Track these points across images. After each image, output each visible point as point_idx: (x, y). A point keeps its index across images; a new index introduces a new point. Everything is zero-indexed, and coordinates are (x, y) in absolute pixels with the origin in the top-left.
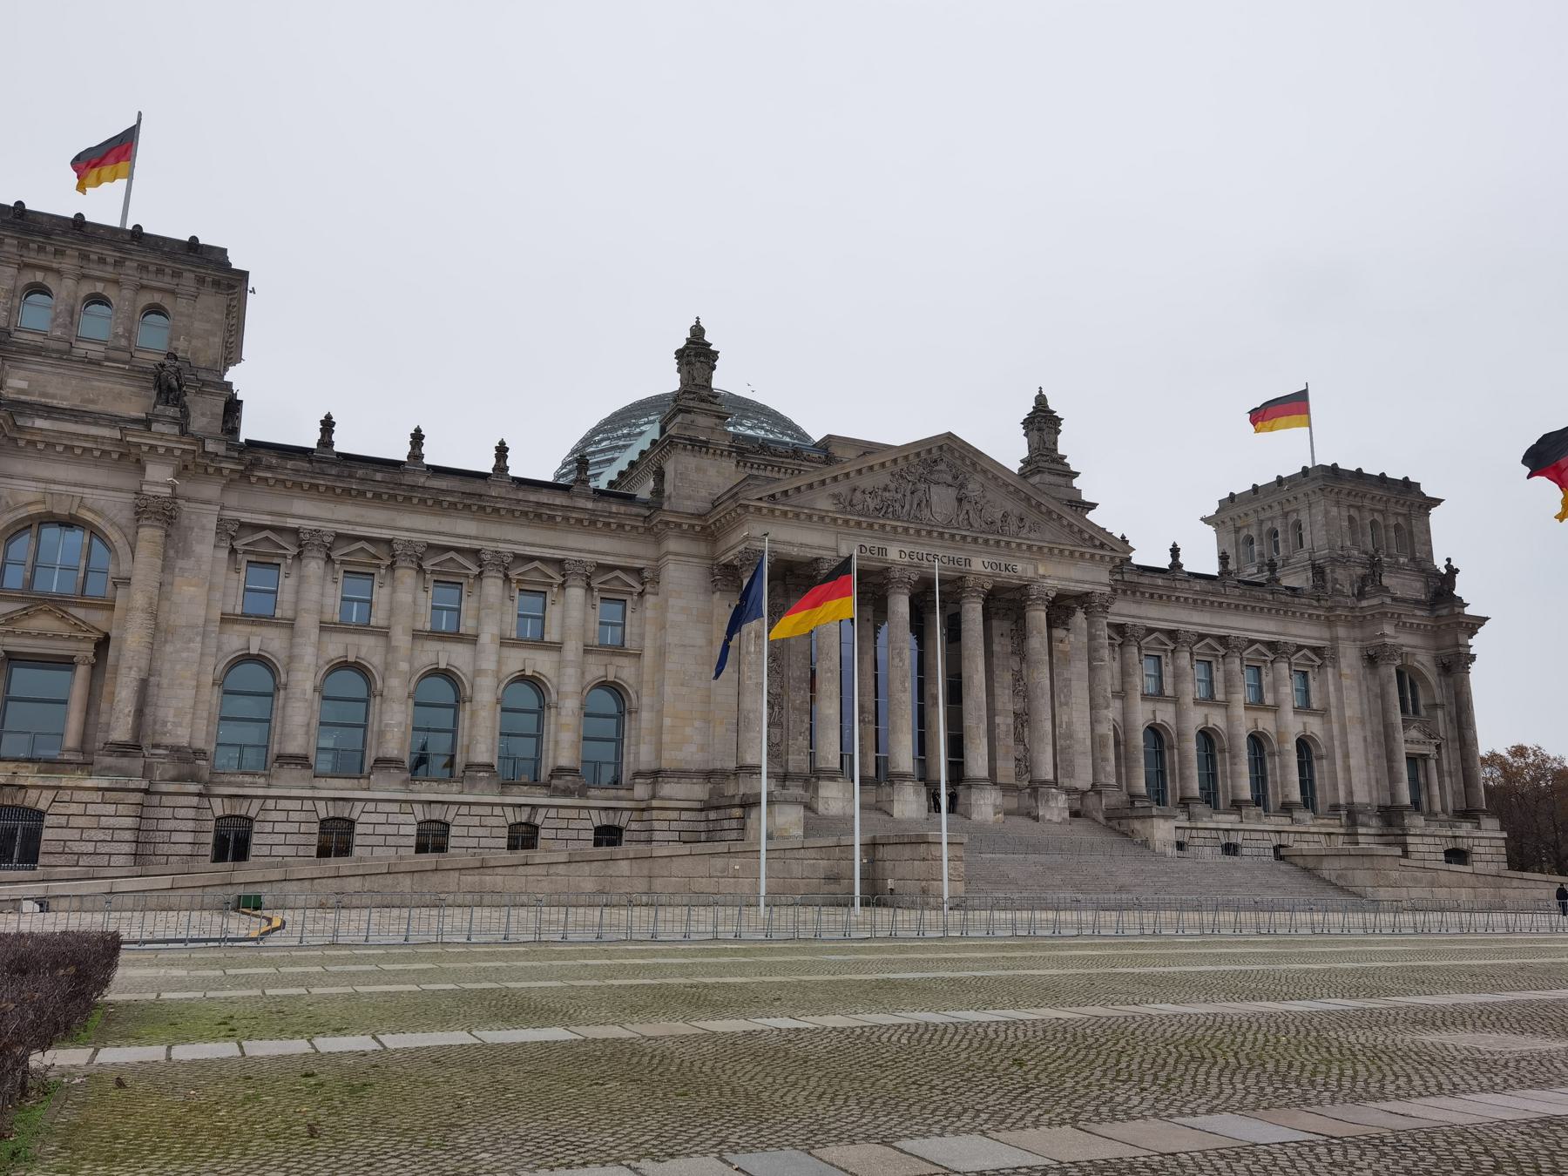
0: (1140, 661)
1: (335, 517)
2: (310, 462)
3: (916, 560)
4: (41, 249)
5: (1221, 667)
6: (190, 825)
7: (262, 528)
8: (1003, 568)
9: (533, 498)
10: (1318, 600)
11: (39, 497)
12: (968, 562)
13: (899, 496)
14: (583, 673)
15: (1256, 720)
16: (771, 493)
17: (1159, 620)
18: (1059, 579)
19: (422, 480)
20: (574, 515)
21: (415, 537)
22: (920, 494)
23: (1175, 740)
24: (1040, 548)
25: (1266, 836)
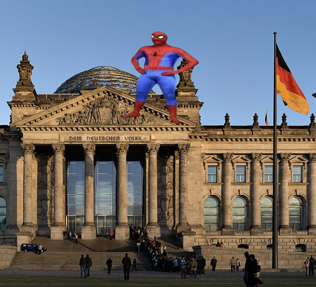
0: (233, 169)
3: (94, 140)
8: (135, 138)
15: (296, 191)
17: (242, 150)
18: (162, 140)
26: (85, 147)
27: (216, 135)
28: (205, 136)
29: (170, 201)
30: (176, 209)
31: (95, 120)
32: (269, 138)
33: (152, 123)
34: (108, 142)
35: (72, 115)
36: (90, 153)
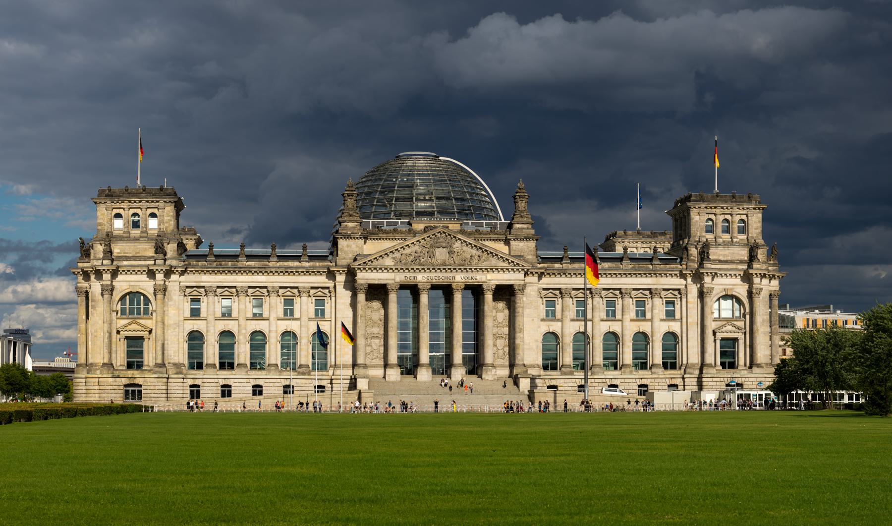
0: (573, 304)
1: (216, 280)
3: (430, 280)
4: (117, 202)
6: (182, 388)
7: (192, 287)
8: (470, 278)
9: (286, 264)
10: (681, 265)
11: (128, 287)
13: (422, 254)
18: (498, 280)
19: (245, 262)
20: (300, 270)
21: (244, 284)
22: (429, 253)
25: (634, 380)
26: (420, 287)
28: (541, 272)
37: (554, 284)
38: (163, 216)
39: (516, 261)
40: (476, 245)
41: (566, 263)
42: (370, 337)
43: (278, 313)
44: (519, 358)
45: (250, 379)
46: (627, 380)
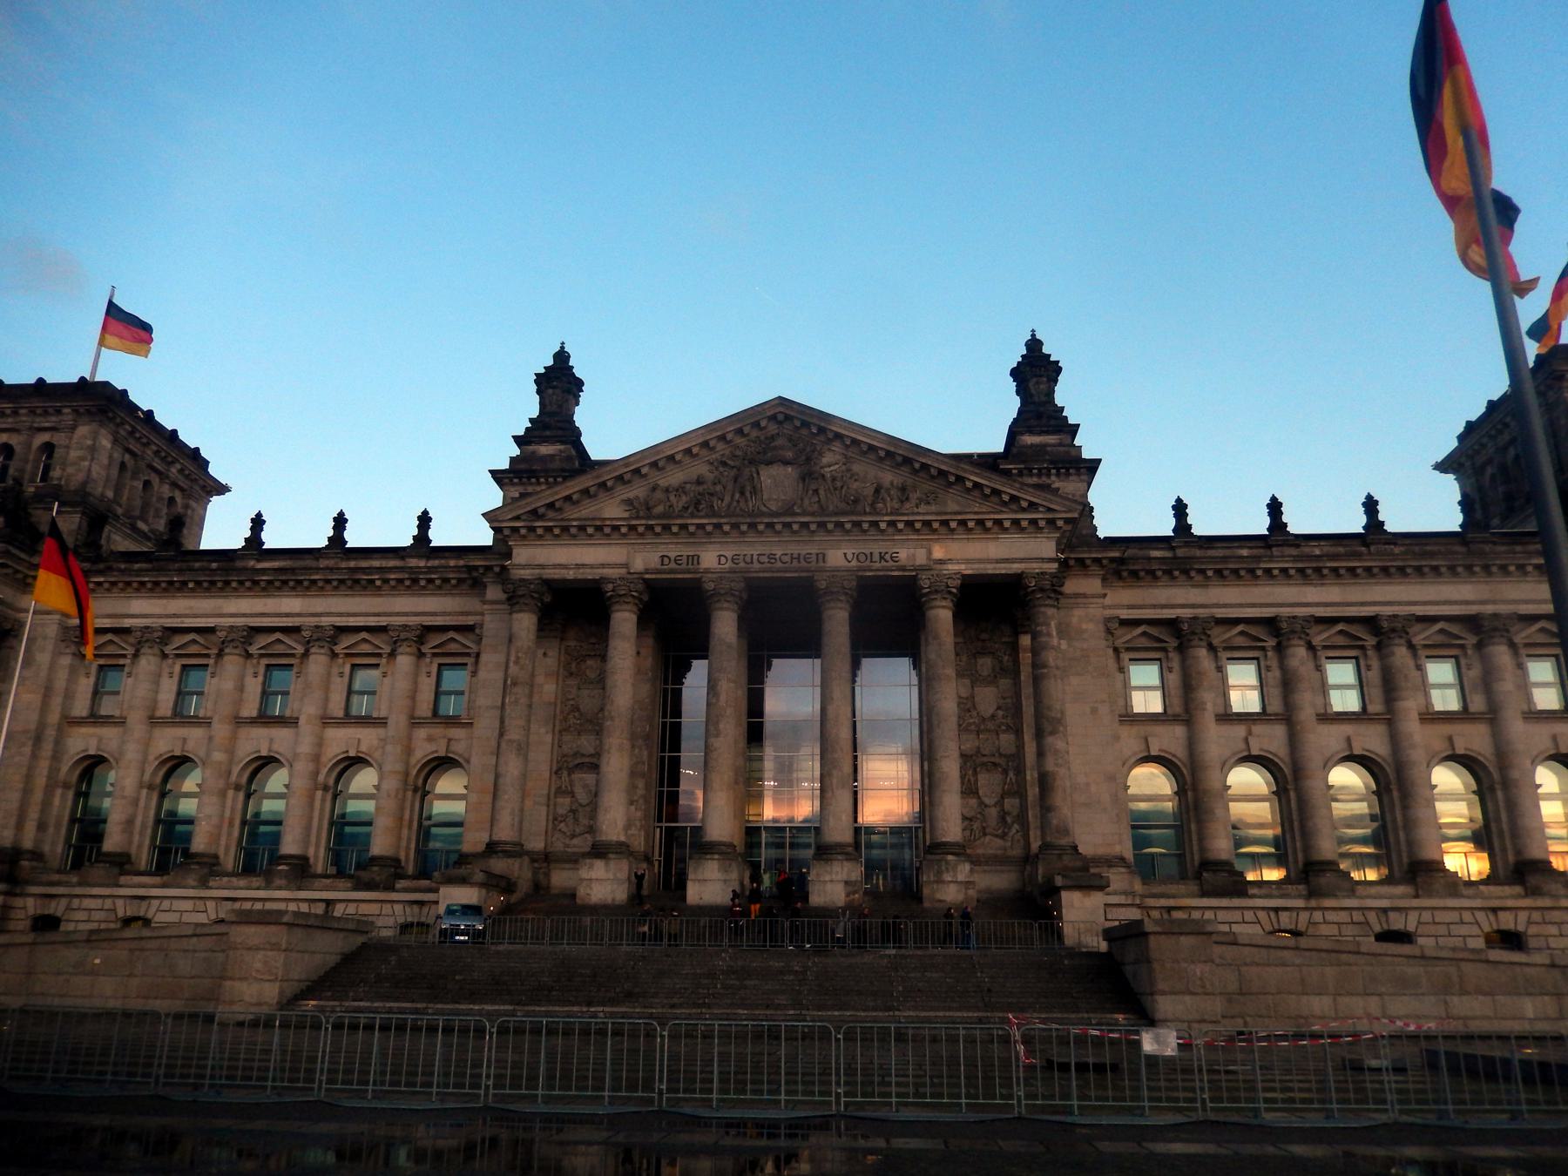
1: (167, 612)
2: (150, 561)
3: (742, 564)
5: (1375, 663)
8: (876, 558)
9: (364, 564)
12: (822, 557)
13: (719, 488)
14: (408, 750)
15: (1450, 739)
16: (534, 506)
17: (1241, 605)
18: (968, 561)
19: (252, 563)
21: (240, 622)
23: (1290, 778)
24: (927, 524)
25: (1467, 916)
26: (710, 586)
27: (1149, 559)
28: (1112, 560)
29: (1005, 772)
30: (1030, 798)
31: (746, 501)
32: (1328, 565)
33: (933, 508)
34: (786, 572)
35: (671, 490)
36: (726, 605)
37: (1154, 606)
38: (67, 447)
39: (1027, 496)
40: (892, 449)
41: (1187, 544)
42: (571, 765)
43: (331, 706)
44: (1055, 822)
45: (208, 903)
46: (1441, 917)
